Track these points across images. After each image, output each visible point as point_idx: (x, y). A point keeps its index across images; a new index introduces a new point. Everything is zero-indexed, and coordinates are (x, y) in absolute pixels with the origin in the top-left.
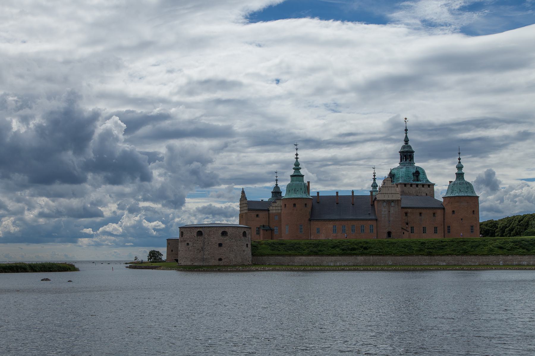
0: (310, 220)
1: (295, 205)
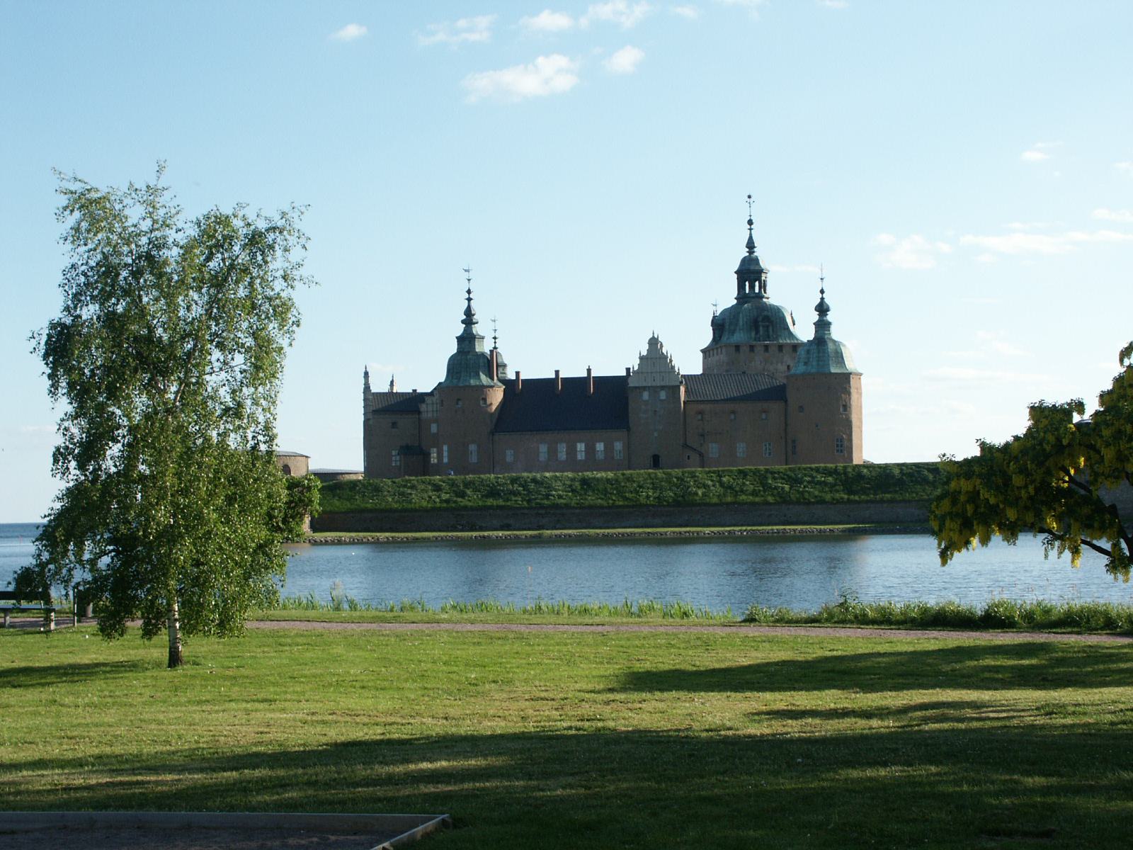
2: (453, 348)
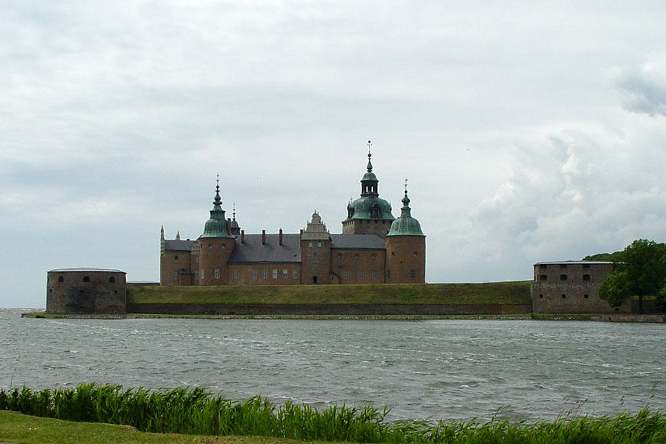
0: (228, 264)
2: (207, 217)
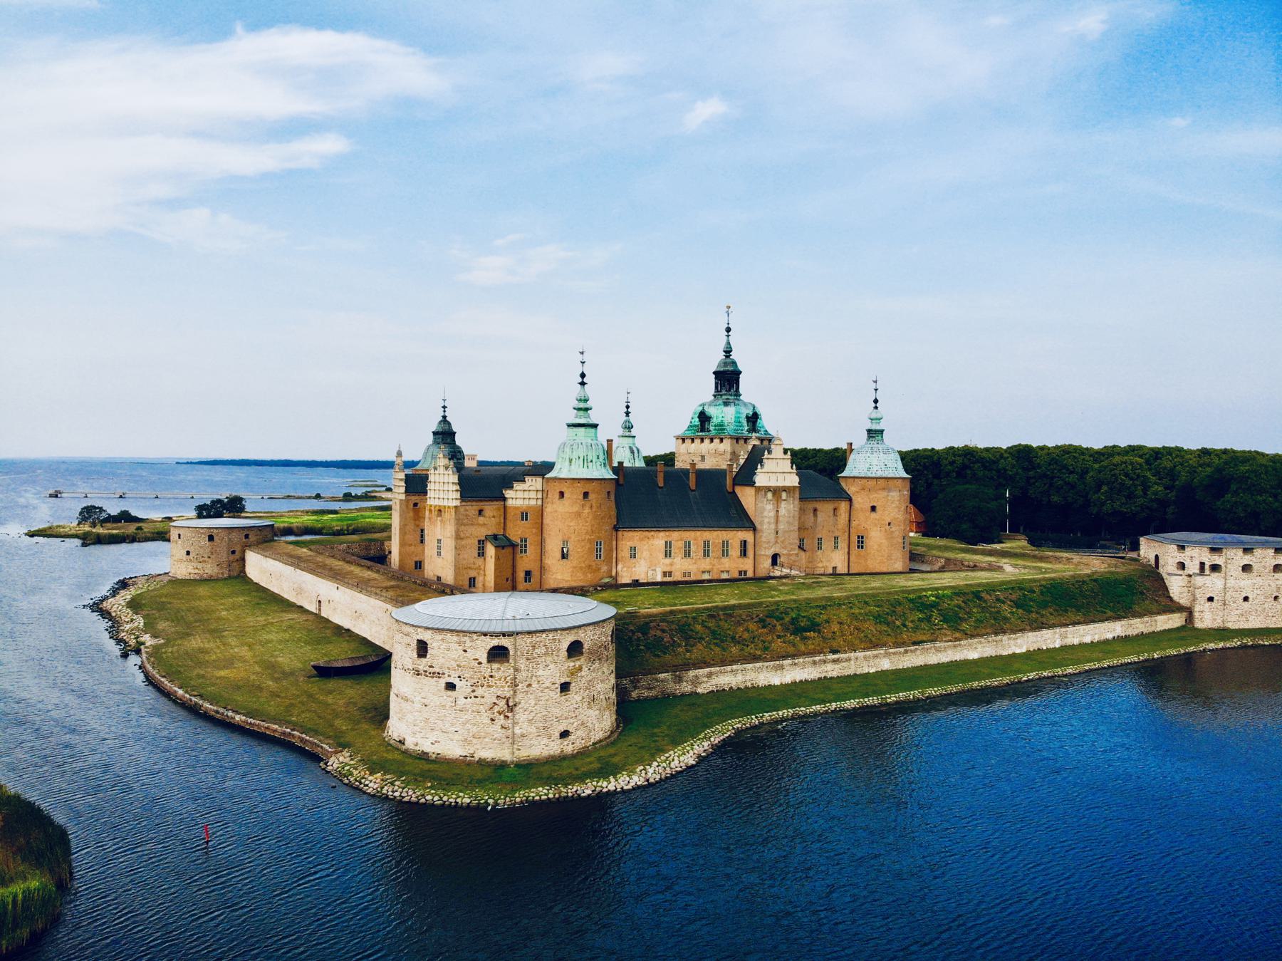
1: (586, 495)
